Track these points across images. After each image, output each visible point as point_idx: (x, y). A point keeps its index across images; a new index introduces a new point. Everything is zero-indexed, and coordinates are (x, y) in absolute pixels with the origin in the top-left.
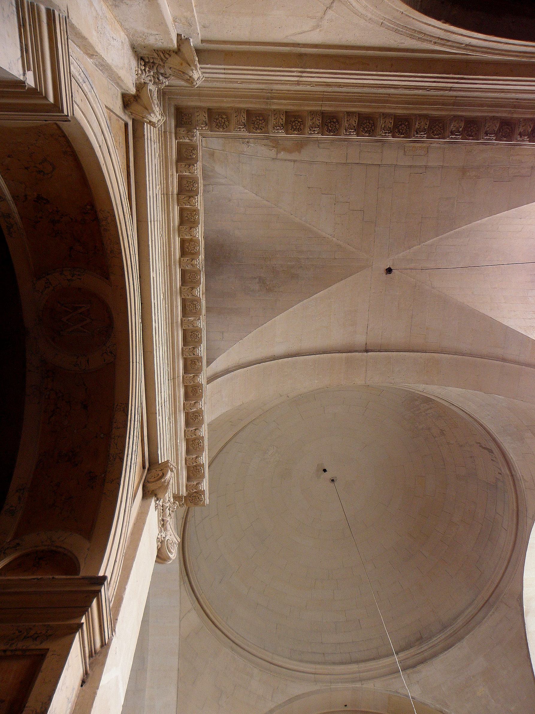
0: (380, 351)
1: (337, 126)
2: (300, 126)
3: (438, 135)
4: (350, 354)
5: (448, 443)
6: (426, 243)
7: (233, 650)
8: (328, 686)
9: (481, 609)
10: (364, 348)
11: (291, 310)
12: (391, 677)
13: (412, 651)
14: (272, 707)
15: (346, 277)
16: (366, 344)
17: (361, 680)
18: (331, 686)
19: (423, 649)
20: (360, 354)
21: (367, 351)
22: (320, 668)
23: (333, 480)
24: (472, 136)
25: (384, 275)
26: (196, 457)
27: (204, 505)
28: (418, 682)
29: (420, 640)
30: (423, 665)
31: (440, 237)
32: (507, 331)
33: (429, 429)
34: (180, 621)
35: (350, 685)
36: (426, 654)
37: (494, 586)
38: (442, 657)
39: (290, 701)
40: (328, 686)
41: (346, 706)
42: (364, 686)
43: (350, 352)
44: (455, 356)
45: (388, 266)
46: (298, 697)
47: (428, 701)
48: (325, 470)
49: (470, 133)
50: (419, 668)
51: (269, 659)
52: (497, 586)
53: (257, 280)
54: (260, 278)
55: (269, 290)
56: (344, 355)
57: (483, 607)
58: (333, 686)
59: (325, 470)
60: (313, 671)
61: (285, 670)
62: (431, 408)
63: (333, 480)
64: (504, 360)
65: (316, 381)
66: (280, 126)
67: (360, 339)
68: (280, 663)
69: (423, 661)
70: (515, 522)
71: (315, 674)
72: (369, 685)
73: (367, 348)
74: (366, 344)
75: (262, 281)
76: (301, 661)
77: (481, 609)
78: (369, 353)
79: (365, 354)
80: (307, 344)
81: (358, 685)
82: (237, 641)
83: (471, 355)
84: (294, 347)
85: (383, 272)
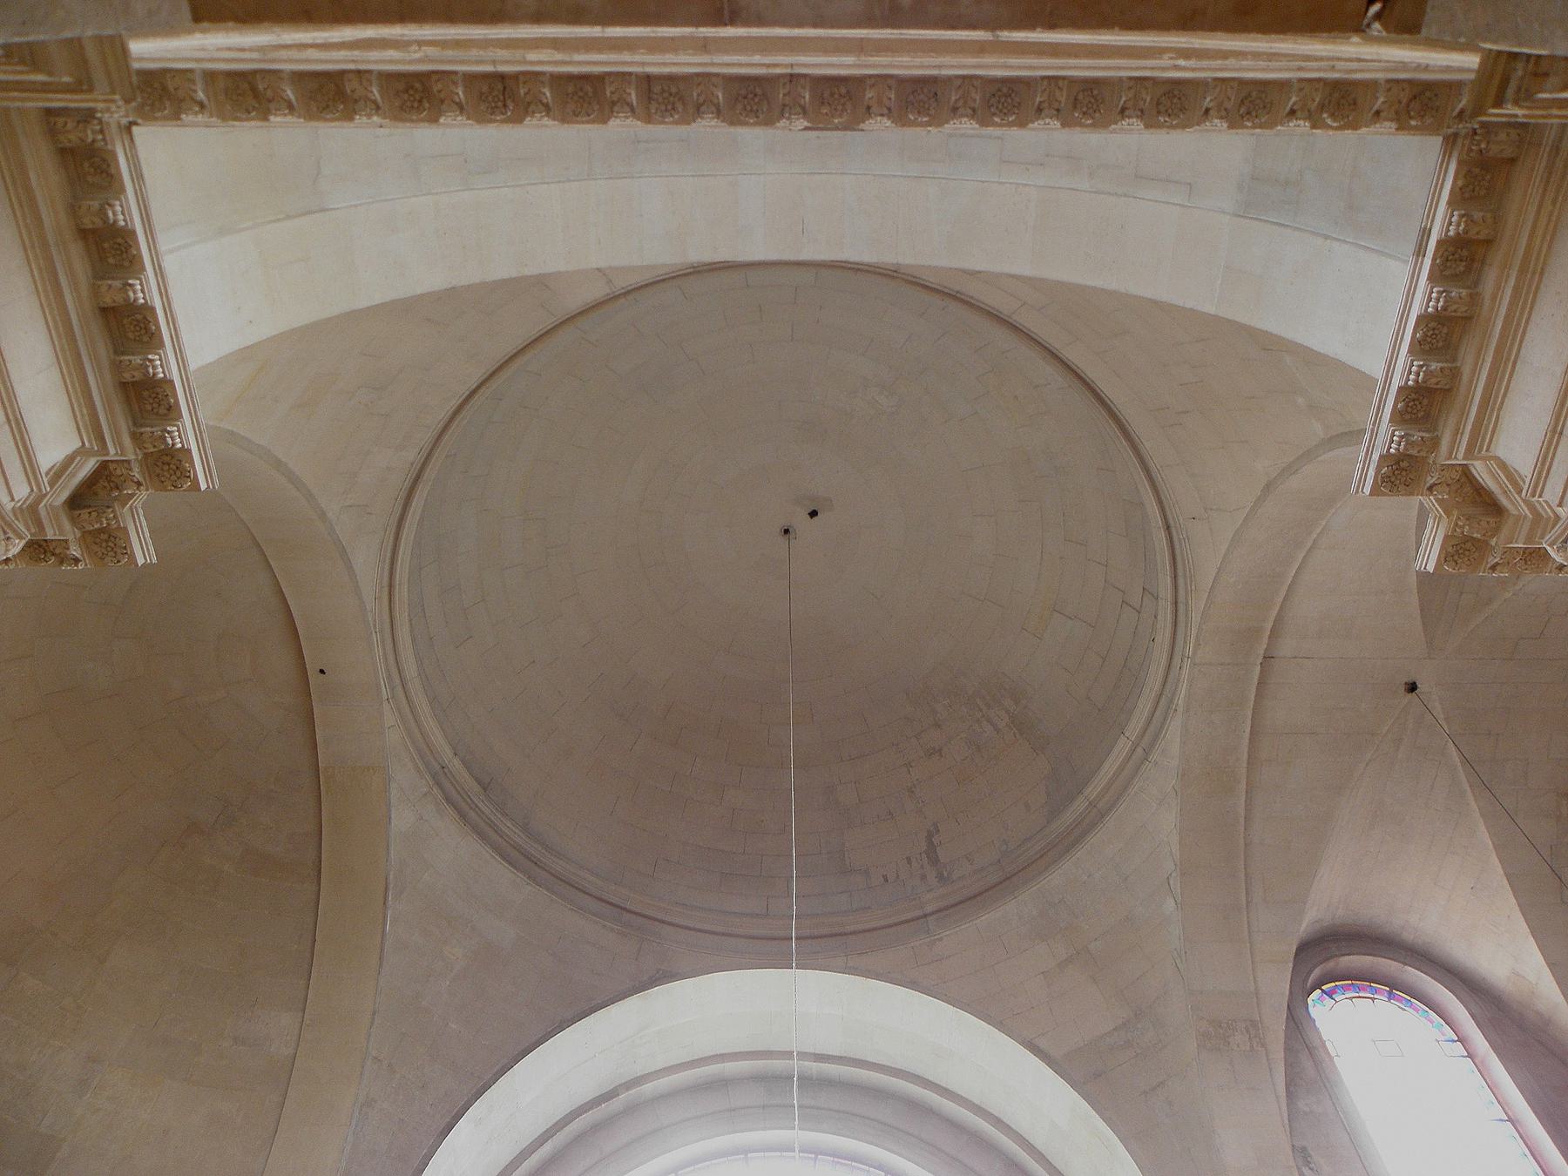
8: (375, 625)
14: (330, 515)
16: (1273, 657)
19: (480, 805)
25: (1406, 680)
33: (937, 725)
36: (472, 814)
37: (660, 916)
40: (375, 625)
41: (322, 671)
48: (813, 514)
50: (450, 810)
56: (1269, 625)
57: (611, 904)
62: (998, 731)
67: (1286, 647)
69: (463, 815)
70: (816, 932)
74: (1273, 657)
85: (1410, 680)
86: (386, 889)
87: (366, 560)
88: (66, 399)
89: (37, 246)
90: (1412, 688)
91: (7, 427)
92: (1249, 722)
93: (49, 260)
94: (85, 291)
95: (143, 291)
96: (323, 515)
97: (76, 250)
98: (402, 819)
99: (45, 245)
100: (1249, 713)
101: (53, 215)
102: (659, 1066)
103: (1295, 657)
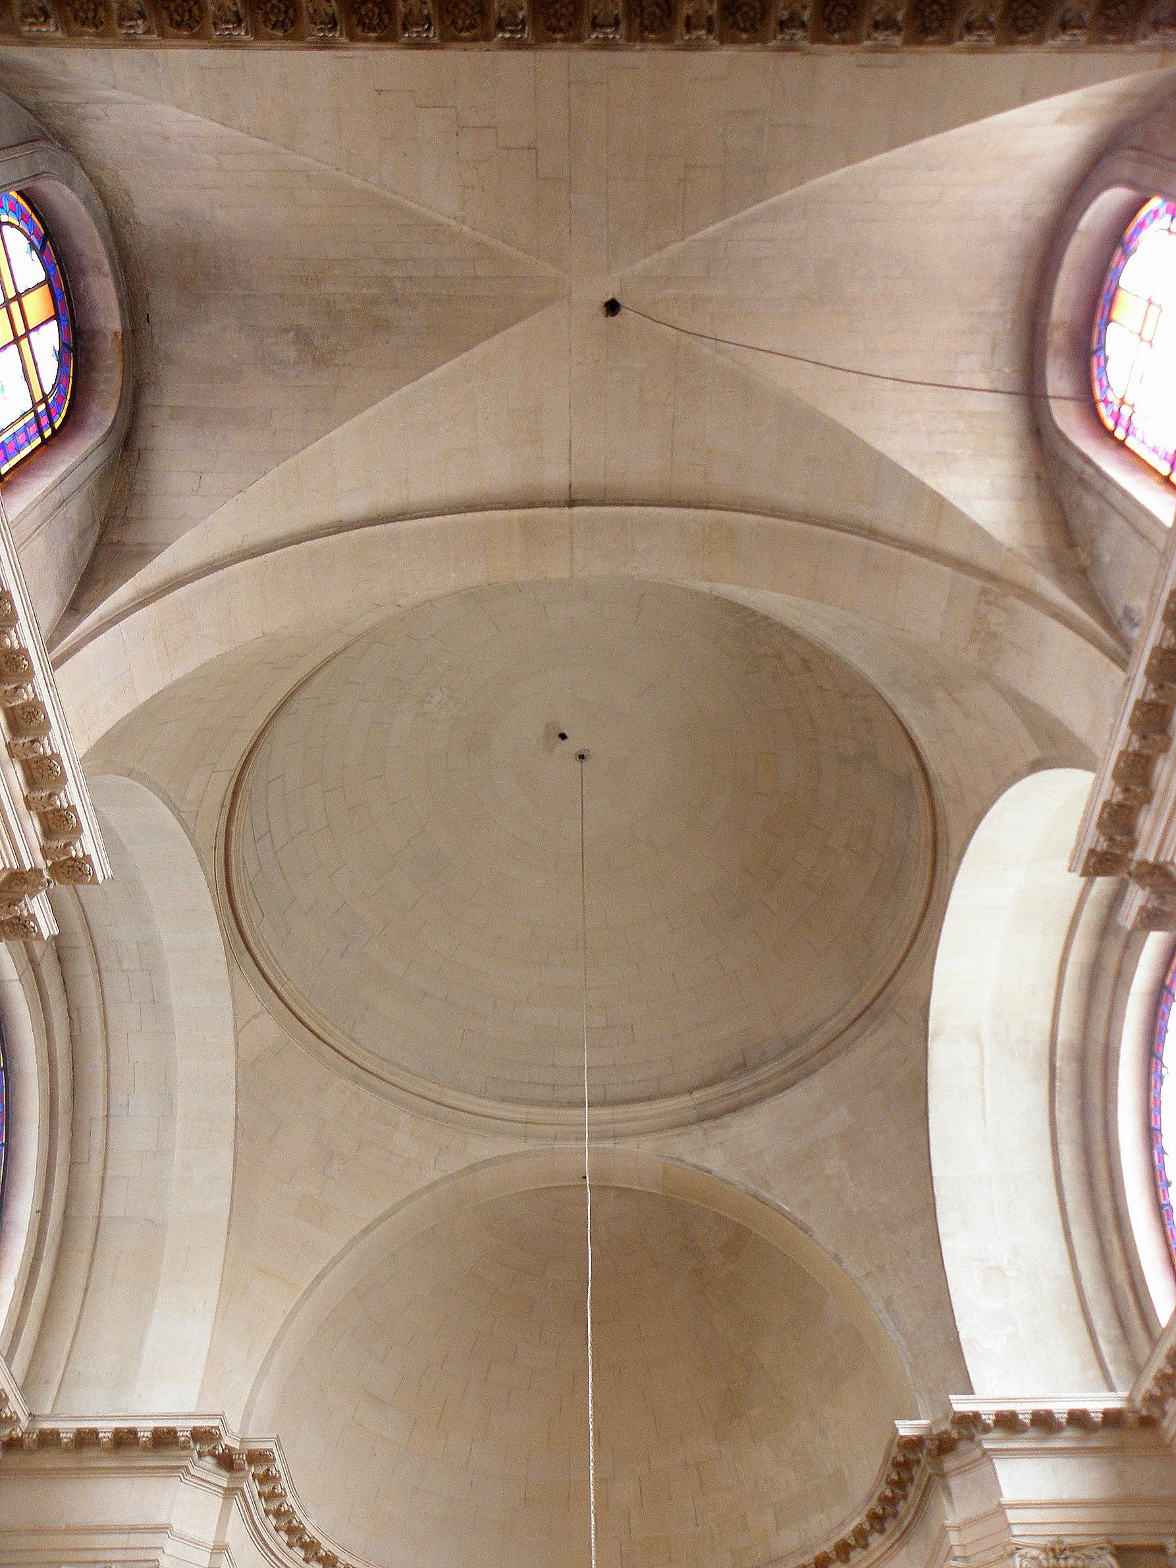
0: (602, 503)
1: (195, 10)
2: (96, 11)
3: (468, 29)
4: (529, 512)
5: (820, 688)
6: (700, 235)
7: (356, 1080)
9: (856, 1020)
10: (565, 497)
11: (370, 412)
12: (670, 1132)
13: (719, 1089)
14: (436, 1178)
15: (507, 326)
16: (570, 486)
17: (615, 1136)
18: (554, 1144)
19: (740, 1087)
20: (555, 511)
21: (571, 503)
22: (537, 1113)
23: (582, 757)
24: (561, 30)
25: (602, 318)
26: (50, 796)
27: (94, 881)
29: (742, 1067)
30: (733, 1115)
31: (732, 218)
32: (881, 465)
33: (779, 656)
34: (237, 1033)
36: (744, 1096)
37: (883, 981)
38: (772, 1102)
39: (472, 1168)
43: (532, 505)
44: (770, 520)
45: (610, 297)
46: (488, 1163)
47: (735, 1178)
48: (563, 736)
49: (553, 21)
50: (727, 1119)
51: (436, 1097)
52: (889, 981)
53: (292, 335)
54: (298, 330)
55: (321, 361)
56: (516, 513)
58: (559, 1145)
59: (563, 736)
60: (524, 1117)
63: (582, 757)
64: (872, 533)
66: (37, 12)
68: (456, 1103)
69: (735, 1109)
72: (629, 1146)
73: (574, 496)
74: (570, 486)
75: (303, 337)
76: (504, 1100)
77: (856, 1020)
78: (577, 510)
79: (566, 510)
80: (422, 491)
81: (608, 1145)
82: (367, 1065)
83: (806, 518)
84: (390, 498)
85: (601, 311)
86: (756, 1197)
87: (483, 1148)
89: (80, 1472)
90: (612, 307)
91: (132, 1536)
94: (104, 1454)
95: (105, 1432)
96: (432, 1186)
97: (86, 1452)
98: (715, 1161)
101: (67, 1462)
102: (1047, 1019)
103: (570, 461)
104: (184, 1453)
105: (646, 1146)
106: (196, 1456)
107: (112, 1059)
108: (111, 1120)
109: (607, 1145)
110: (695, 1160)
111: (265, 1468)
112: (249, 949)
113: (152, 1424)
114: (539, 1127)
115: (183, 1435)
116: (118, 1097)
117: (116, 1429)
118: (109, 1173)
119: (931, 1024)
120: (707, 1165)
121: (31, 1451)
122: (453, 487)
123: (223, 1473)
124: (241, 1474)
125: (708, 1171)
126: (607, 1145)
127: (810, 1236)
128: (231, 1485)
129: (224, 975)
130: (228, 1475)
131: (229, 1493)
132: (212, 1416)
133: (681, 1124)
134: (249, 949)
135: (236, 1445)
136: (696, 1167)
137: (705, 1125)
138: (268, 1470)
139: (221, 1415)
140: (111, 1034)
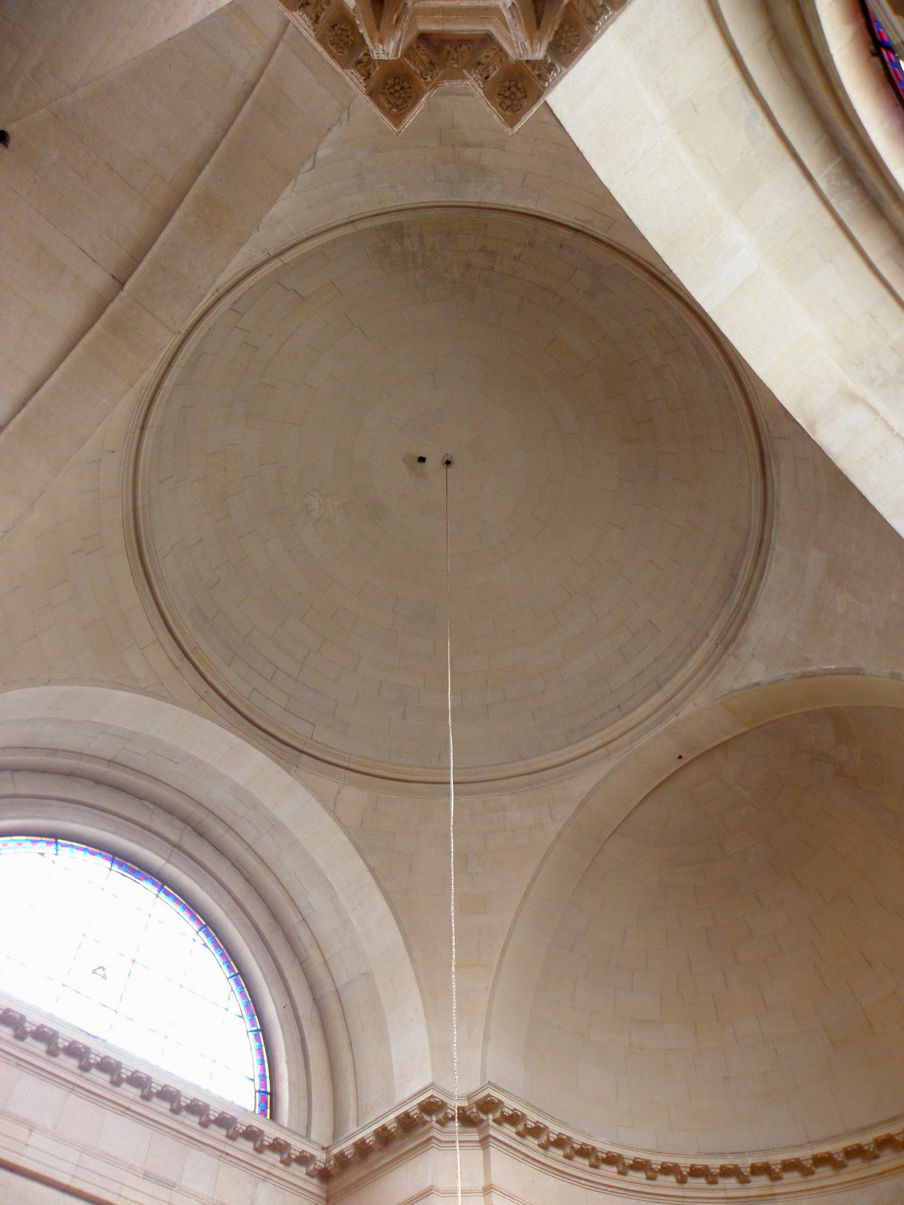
4: (104, 318)
8: (629, 750)
14: (559, 828)
16: (113, 277)
18: (632, 747)
20: (116, 301)
28: (753, 655)
33: (468, 265)
34: (333, 813)
35: (661, 729)
39: (582, 804)
40: (629, 750)
41: (680, 757)
42: (680, 716)
46: (592, 793)
48: (422, 460)
51: (524, 770)
56: (98, 326)
60: (599, 743)
61: (557, 768)
65: (105, 401)
68: (542, 765)
71: (604, 745)
72: (688, 709)
74: (113, 277)
80: (34, 366)
81: (672, 719)
86: (804, 676)
87: (582, 784)
88: (419, 1157)
89: (375, 1175)
92: (161, 240)
93: (376, 1170)
97: (372, 1158)
98: (757, 673)
99: (373, 1172)
100: (155, 249)
101: (363, 1171)
103: (94, 261)
104: (426, 1127)
105: (701, 700)
106: (438, 1126)
107: (282, 880)
108: (308, 920)
109: (672, 721)
110: (743, 683)
111: (499, 1111)
112: (301, 752)
113: (392, 1116)
114: (613, 744)
115: (415, 1113)
116: (301, 903)
117: (375, 1131)
118: (327, 956)
119: (799, 421)
120: (755, 680)
121: (339, 1174)
122: (50, 345)
123: (471, 1129)
124: (484, 1124)
125: (757, 684)
126: (672, 721)
127: (863, 674)
128: (482, 1136)
129: (289, 779)
130: (475, 1130)
131: (484, 1142)
132: (426, 1089)
133: (714, 663)
134: (301, 752)
135: (465, 1104)
136: (747, 687)
137: (730, 651)
138: (502, 1112)
139: (431, 1086)
140: (269, 864)
